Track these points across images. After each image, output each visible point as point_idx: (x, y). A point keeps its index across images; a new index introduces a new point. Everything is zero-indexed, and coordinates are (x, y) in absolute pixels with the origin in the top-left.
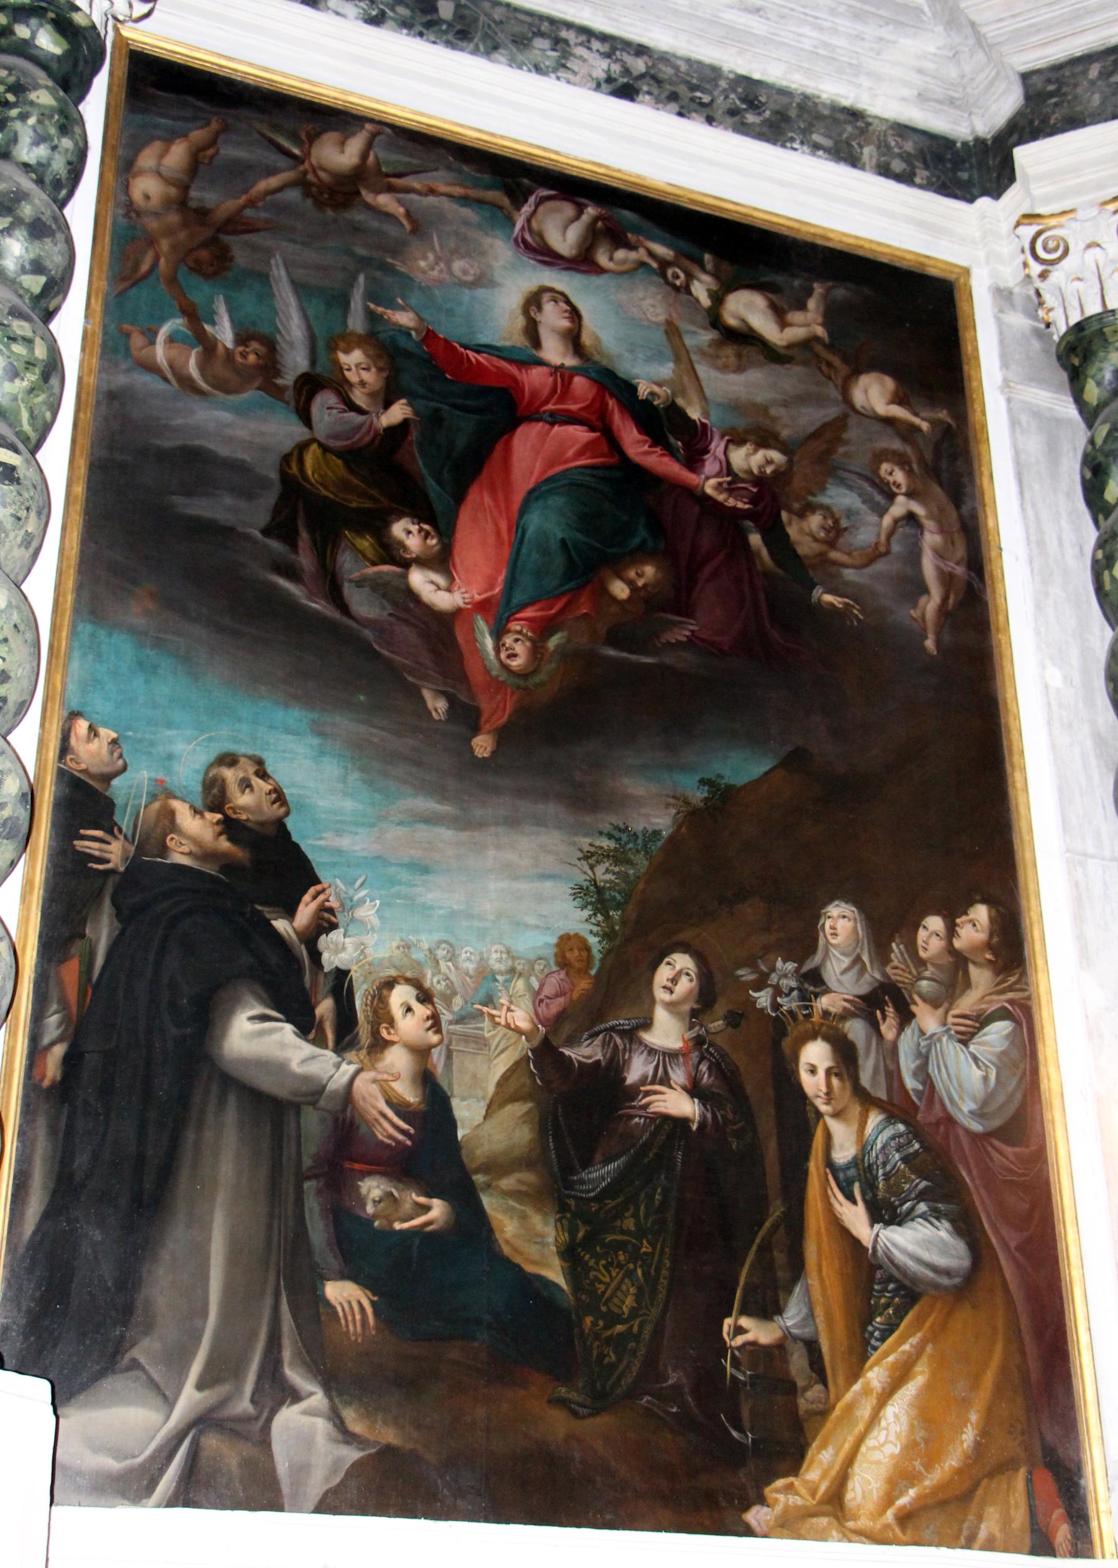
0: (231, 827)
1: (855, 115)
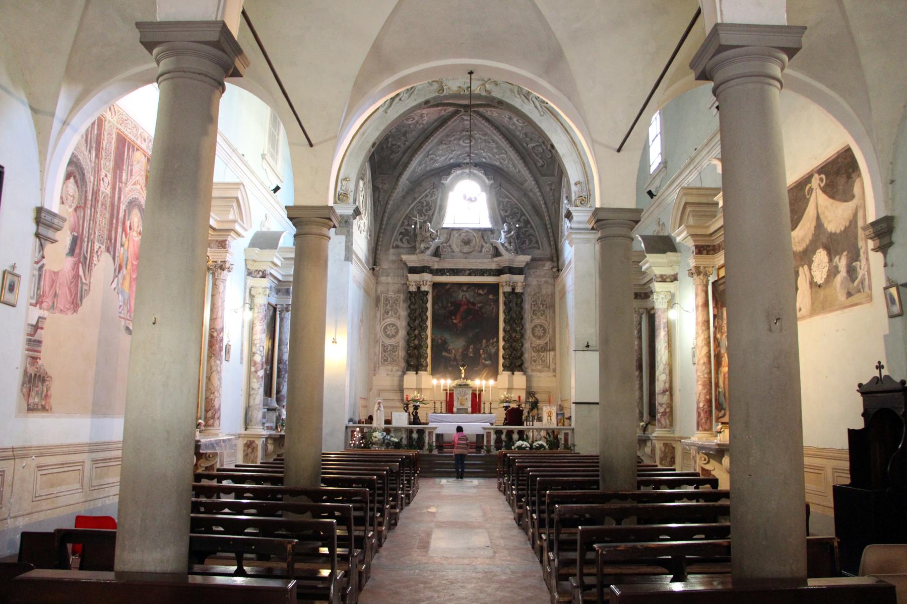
0: (442, 341)
1: (491, 269)
